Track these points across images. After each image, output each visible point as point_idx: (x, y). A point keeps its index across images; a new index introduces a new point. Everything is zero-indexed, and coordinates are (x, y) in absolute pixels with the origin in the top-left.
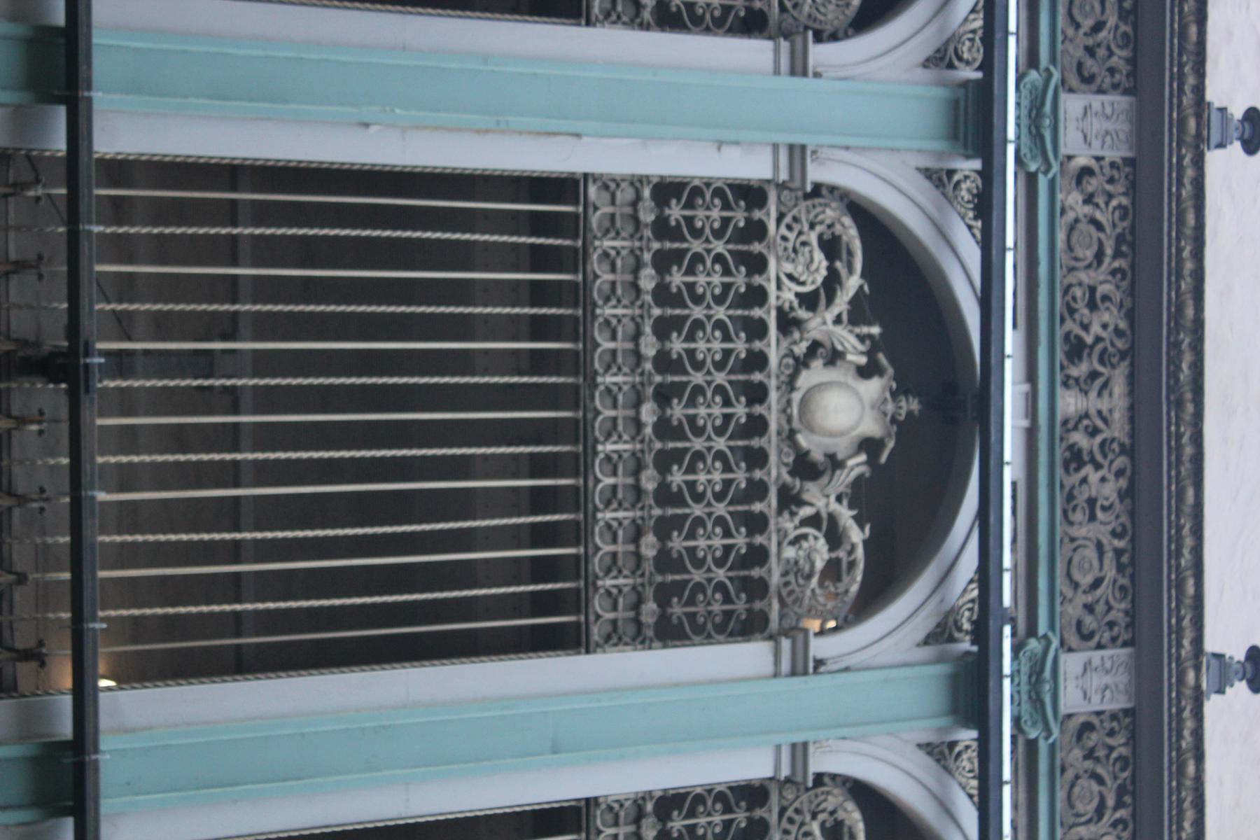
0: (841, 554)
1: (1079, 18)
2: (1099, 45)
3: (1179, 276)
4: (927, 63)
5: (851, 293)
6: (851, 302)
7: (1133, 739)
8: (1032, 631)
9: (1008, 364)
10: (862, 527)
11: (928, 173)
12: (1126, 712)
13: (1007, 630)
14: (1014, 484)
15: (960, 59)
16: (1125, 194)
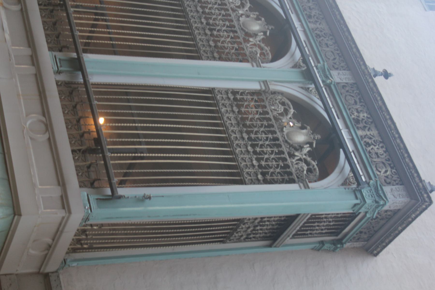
0: (311, 167)
1: (380, 170)
2: (388, 175)
3: (414, 178)
4: (293, 67)
5: (292, 113)
6: (293, 115)
7: (358, 88)
8: (319, 62)
9: (342, 131)
10: (315, 162)
11: (293, 67)
12: (354, 84)
13: (310, 58)
14: (305, 41)
15: (351, 183)
16: (357, 90)
